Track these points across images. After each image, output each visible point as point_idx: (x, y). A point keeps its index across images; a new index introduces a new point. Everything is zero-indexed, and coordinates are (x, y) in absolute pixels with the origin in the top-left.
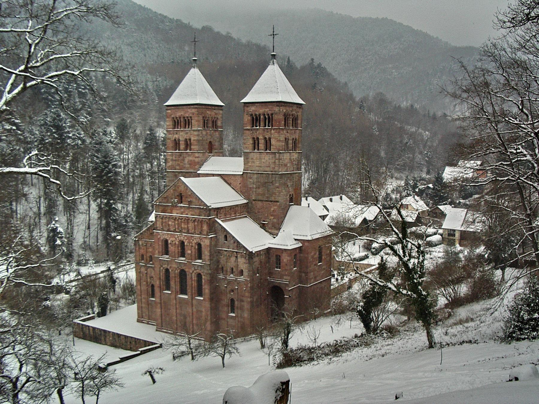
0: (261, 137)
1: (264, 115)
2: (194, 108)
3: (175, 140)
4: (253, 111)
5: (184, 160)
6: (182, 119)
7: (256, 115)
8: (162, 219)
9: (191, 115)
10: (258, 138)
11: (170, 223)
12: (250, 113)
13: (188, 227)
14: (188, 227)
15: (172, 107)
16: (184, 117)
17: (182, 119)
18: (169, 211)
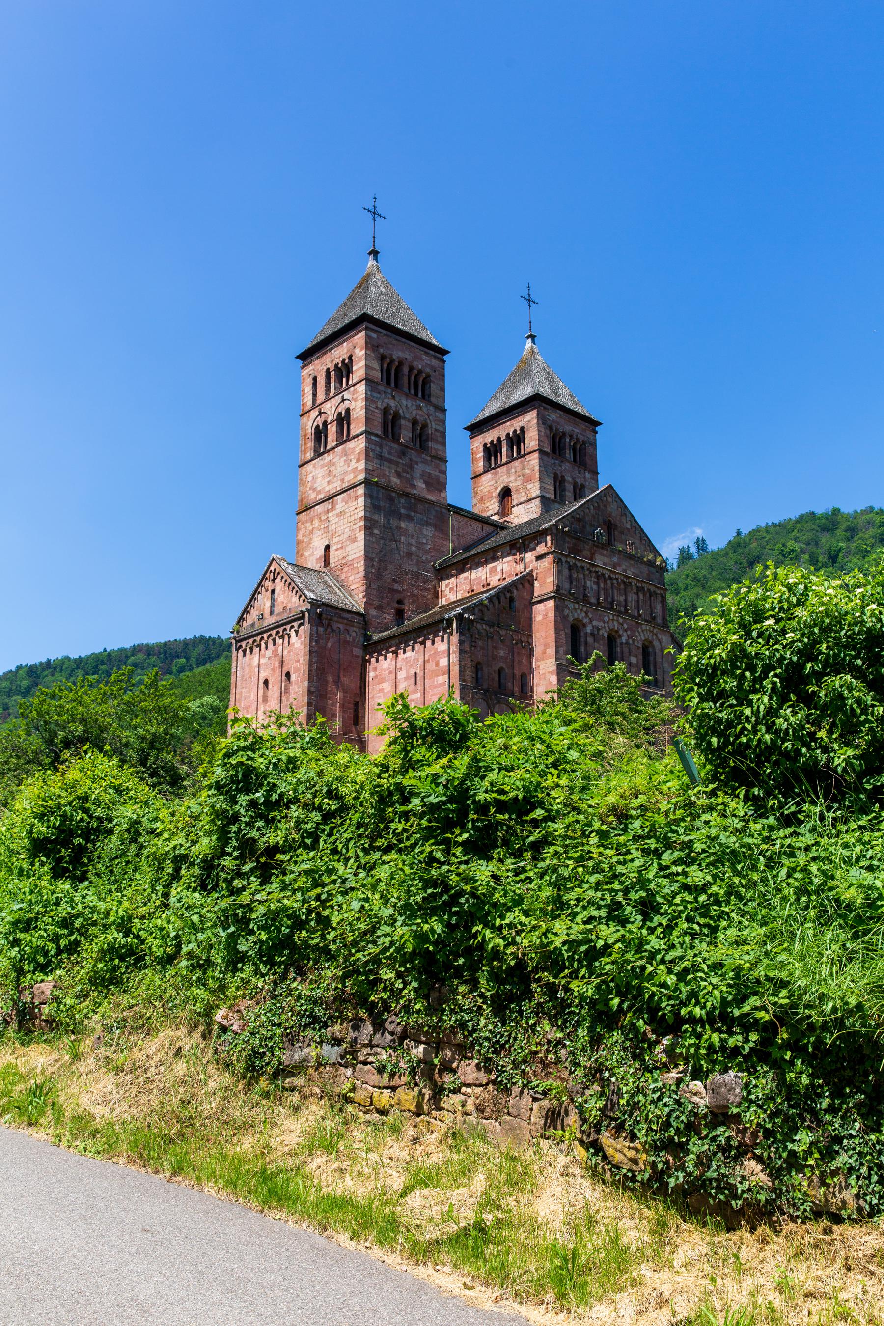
0: (568, 478)
1: (571, 436)
2: (436, 357)
3: (386, 411)
4: (553, 421)
5: (412, 467)
6: (406, 370)
7: (557, 430)
8: (570, 568)
9: (428, 370)
10: (563, 477)
11: (588, 584)
12: (549, 423)
13: (626, 600)
14: (626, 600)
15: (384, 332)
16: (411, 369)
17: (406, 370)
18: (586, 553)
